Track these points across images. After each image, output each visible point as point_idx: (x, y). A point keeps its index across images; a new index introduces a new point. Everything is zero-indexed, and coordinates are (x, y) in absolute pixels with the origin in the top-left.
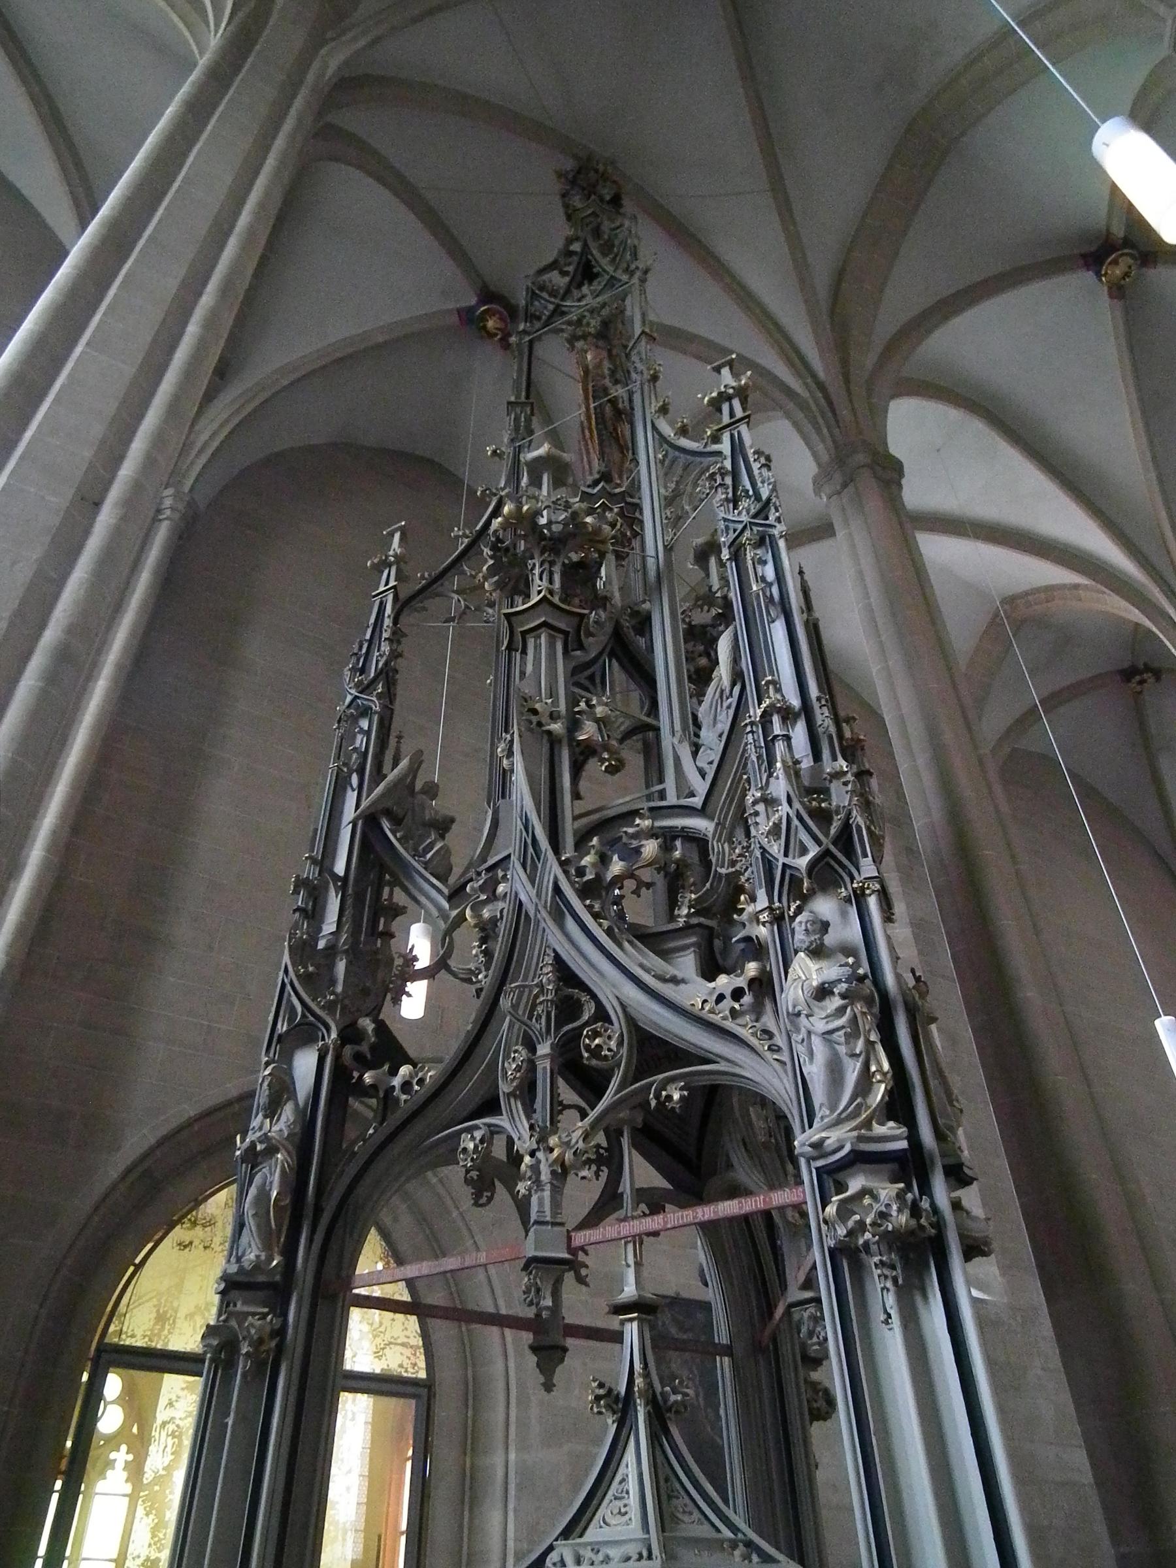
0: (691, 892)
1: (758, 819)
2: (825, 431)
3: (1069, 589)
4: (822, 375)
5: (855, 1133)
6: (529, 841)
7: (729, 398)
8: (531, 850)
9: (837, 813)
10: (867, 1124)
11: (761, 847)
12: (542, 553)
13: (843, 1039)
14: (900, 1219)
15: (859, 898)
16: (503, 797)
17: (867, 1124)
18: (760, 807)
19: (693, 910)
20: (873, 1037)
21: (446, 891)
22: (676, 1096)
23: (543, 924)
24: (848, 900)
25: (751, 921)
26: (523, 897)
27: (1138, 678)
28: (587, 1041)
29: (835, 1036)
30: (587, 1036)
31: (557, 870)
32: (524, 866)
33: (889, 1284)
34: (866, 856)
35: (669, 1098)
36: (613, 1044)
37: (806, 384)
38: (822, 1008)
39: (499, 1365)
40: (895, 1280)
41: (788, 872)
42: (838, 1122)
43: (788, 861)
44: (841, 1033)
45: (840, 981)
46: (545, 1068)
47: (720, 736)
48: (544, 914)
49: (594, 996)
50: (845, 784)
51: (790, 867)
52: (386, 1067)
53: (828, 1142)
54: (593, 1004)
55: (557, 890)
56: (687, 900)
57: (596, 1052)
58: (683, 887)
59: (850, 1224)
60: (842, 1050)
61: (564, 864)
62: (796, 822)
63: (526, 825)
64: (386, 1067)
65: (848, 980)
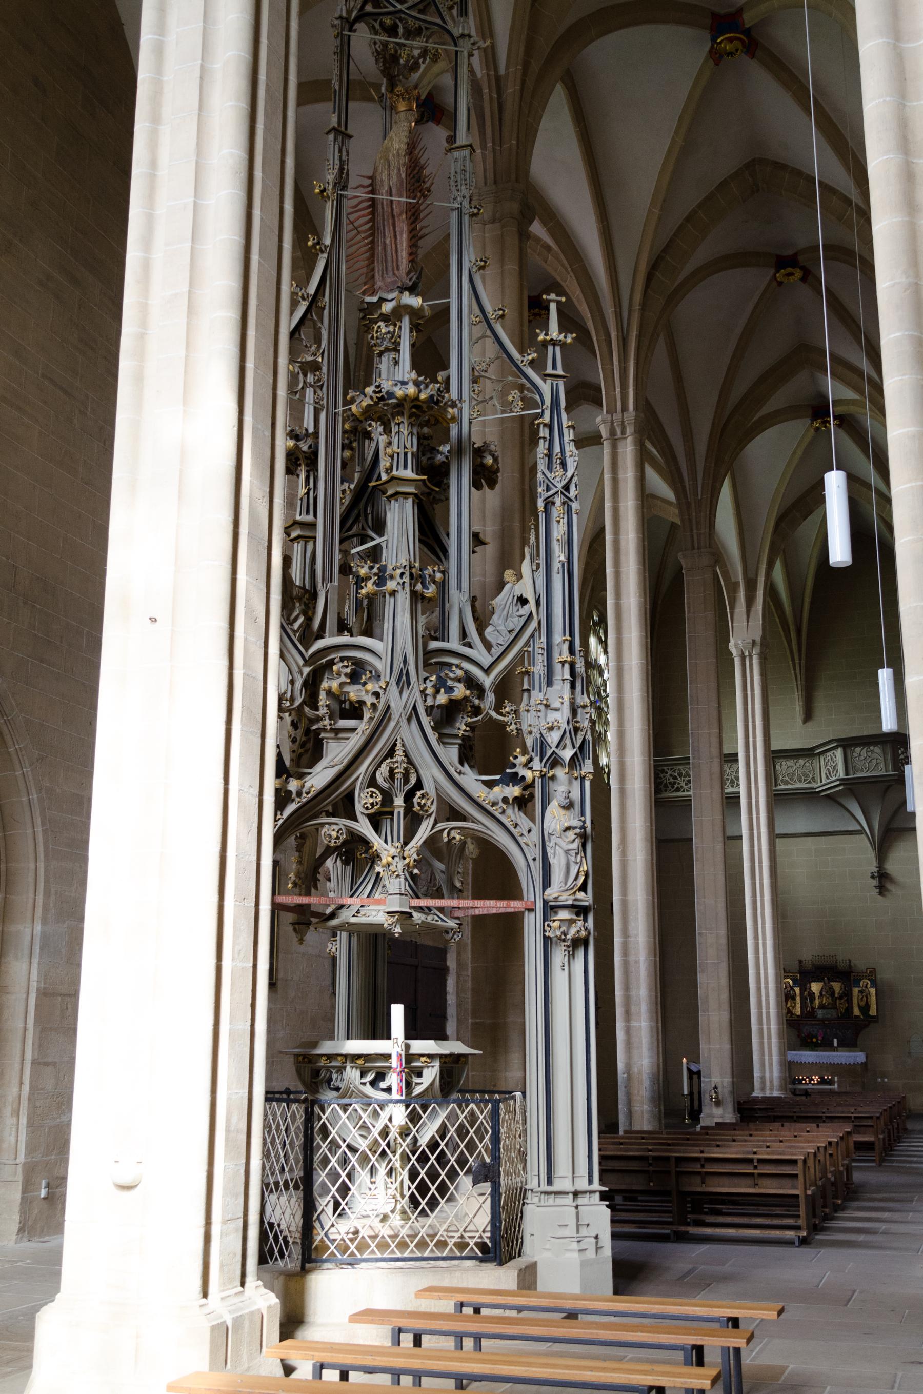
0: (468, 716)
1: (539, 714)
2: (490, 145)
3: (542, 246)
4: (502, 71)
5: (573, 897)
6: (404, 672)
7: (554, 345)
8: (404, 677)
9: (582, 731)
10: (575, 893)
11: (541, 733)
12: (410, 417)
13: (574, 855)
14: (583, 934)
15: (583, 779)
16: (331, 582)
17: (575, 893)
18: (542, 708)
19: (468, 729)
20: (583, 855)
21: (307, 657)
22: (458, 837)
23: (401, 724)
24: (576, 778)
25: (520, 765)
26: (392, 705)
27: (537, 311)
28: (419, 800)
29: (570, 852)
30: (419, 798)
31: (418, 695)
32: (398, 684)
33: (566, 953)
34: (589, 758)
35: (454, 838)
36: (429, 802)
37: (488, 75)
38: (566, 837)
39: (32, 866)
40: (569, 952)
41: (554, 755)
42: (567, 890)
43: (556, 751)
44: (574, 852)
45: (576, 827)
46: (399, 813)
47: (510, 632)
48: (404, 719)
49: (417, 771)
50: (587, 713)
51: (556, 754)
52: (285, 776)
53: (560, 898)
54: (415, 775)
55: (414, 708)
56: (464, 721)
57: (422, 807)
58: (464, 711)
59: (562, 929)
60: (573, 859)
61: (421, 692)
62: (568, 734)
63: (405, 661)
64: (285, 776)
65: (580, 828)
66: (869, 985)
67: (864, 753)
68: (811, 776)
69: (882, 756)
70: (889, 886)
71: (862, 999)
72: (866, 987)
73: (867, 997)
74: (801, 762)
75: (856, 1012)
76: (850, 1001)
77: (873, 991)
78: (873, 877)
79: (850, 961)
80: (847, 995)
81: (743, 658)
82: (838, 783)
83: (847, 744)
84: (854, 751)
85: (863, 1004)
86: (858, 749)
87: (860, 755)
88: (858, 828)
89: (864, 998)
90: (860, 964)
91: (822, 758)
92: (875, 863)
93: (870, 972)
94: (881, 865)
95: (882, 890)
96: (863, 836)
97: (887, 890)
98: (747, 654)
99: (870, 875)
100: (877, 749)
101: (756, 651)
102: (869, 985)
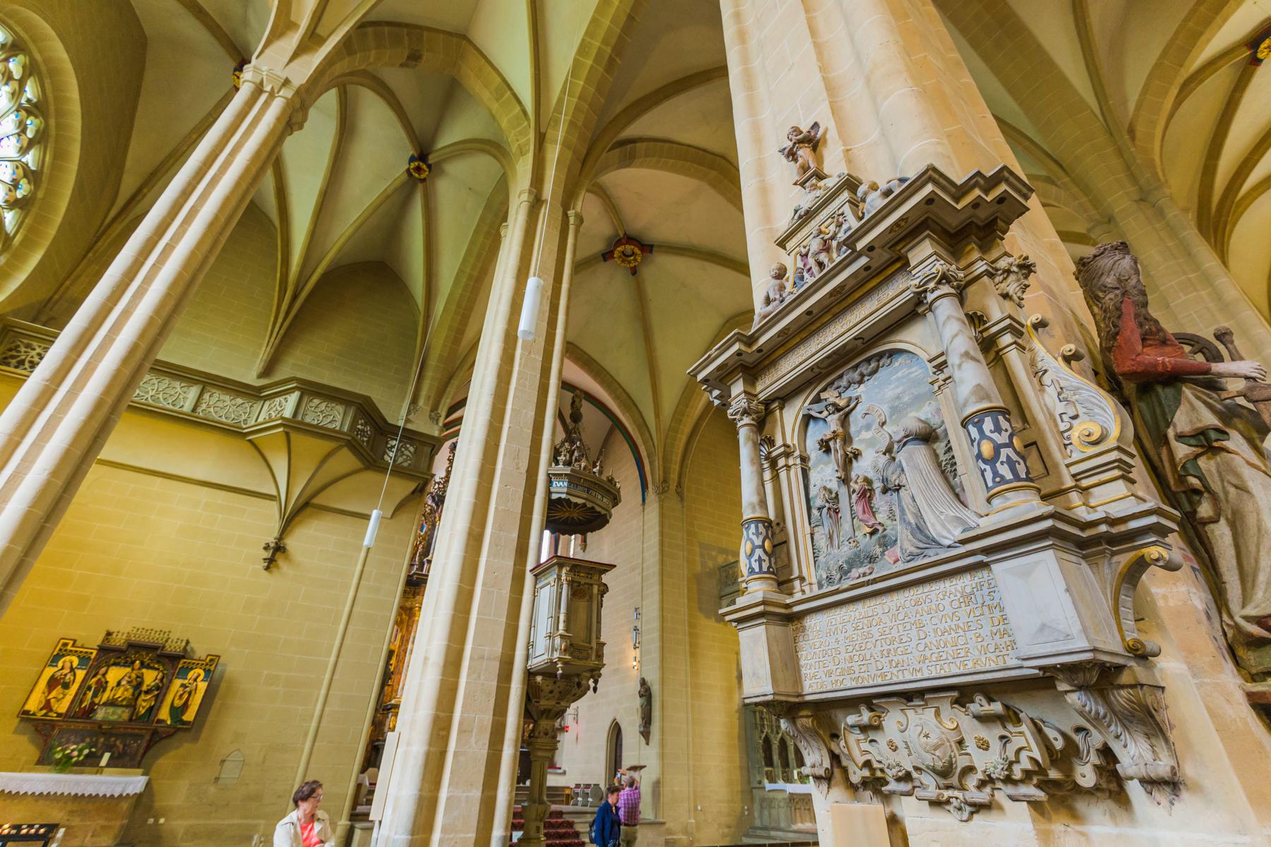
66: (201, 678)
67: (323, 406)
68: (243, 418)
69: (342, 415)
70: (280, 561)
71: (181, 695)
72: (195, 680)
73: (190, 693)
74: (239, 401)
75: (164, 714)
76: (159, 699)
77: (202, 686)
78: (266, 548)
79: (188, 642)
80: (160, 690)
81: (259, 90)
82: (279, 422)
83: (310, 390)
84: (311, 401)
85: (178, 703)
86: (316, 401)
87: (316, 407)
88: (274, 493)
89: (186, 696)
90: (201, 650)
91: (267, 403)
92: (276, 534)
93: (211, 660)
94: (281, 538)
95: (270, 563)
96: (274, 505)
97: (278, 567)
98: (268, 88)
99: (264, 545)
100: (340, 408)
101: (288, 93)
102: (201, 678)
